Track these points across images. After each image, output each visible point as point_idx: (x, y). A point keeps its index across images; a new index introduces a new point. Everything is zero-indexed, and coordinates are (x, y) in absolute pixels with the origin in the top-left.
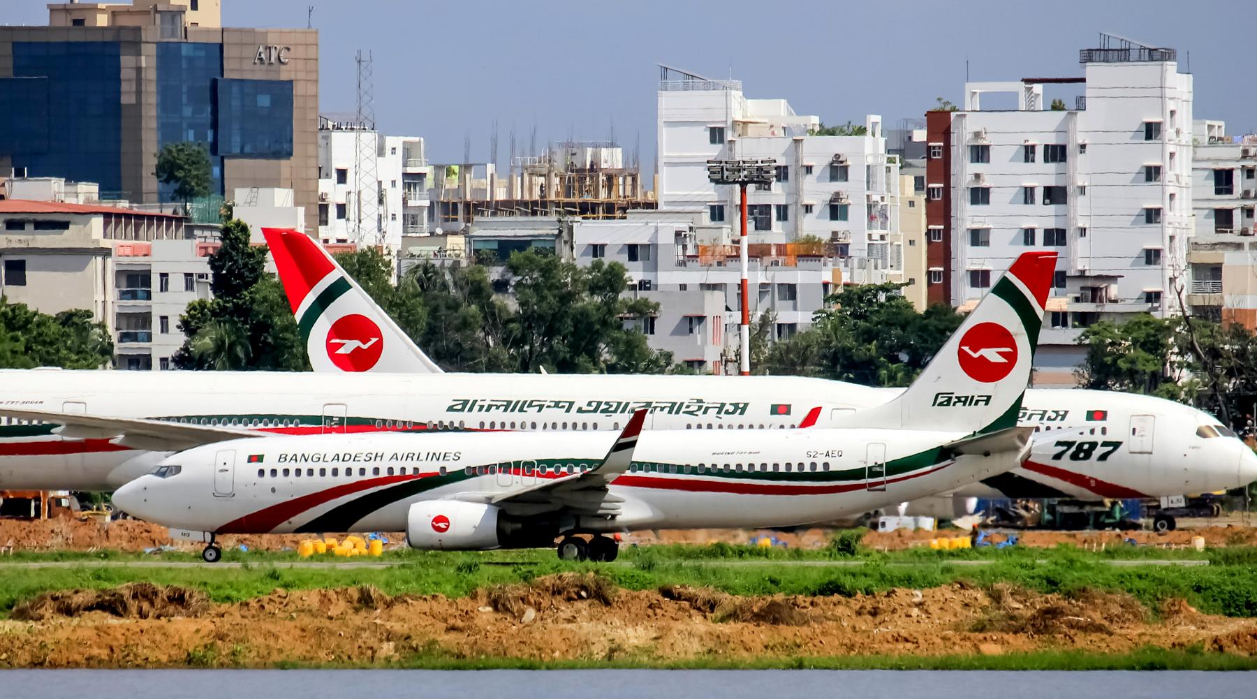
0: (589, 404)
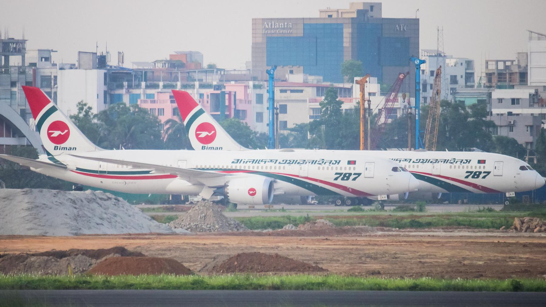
0: (283, 161)
